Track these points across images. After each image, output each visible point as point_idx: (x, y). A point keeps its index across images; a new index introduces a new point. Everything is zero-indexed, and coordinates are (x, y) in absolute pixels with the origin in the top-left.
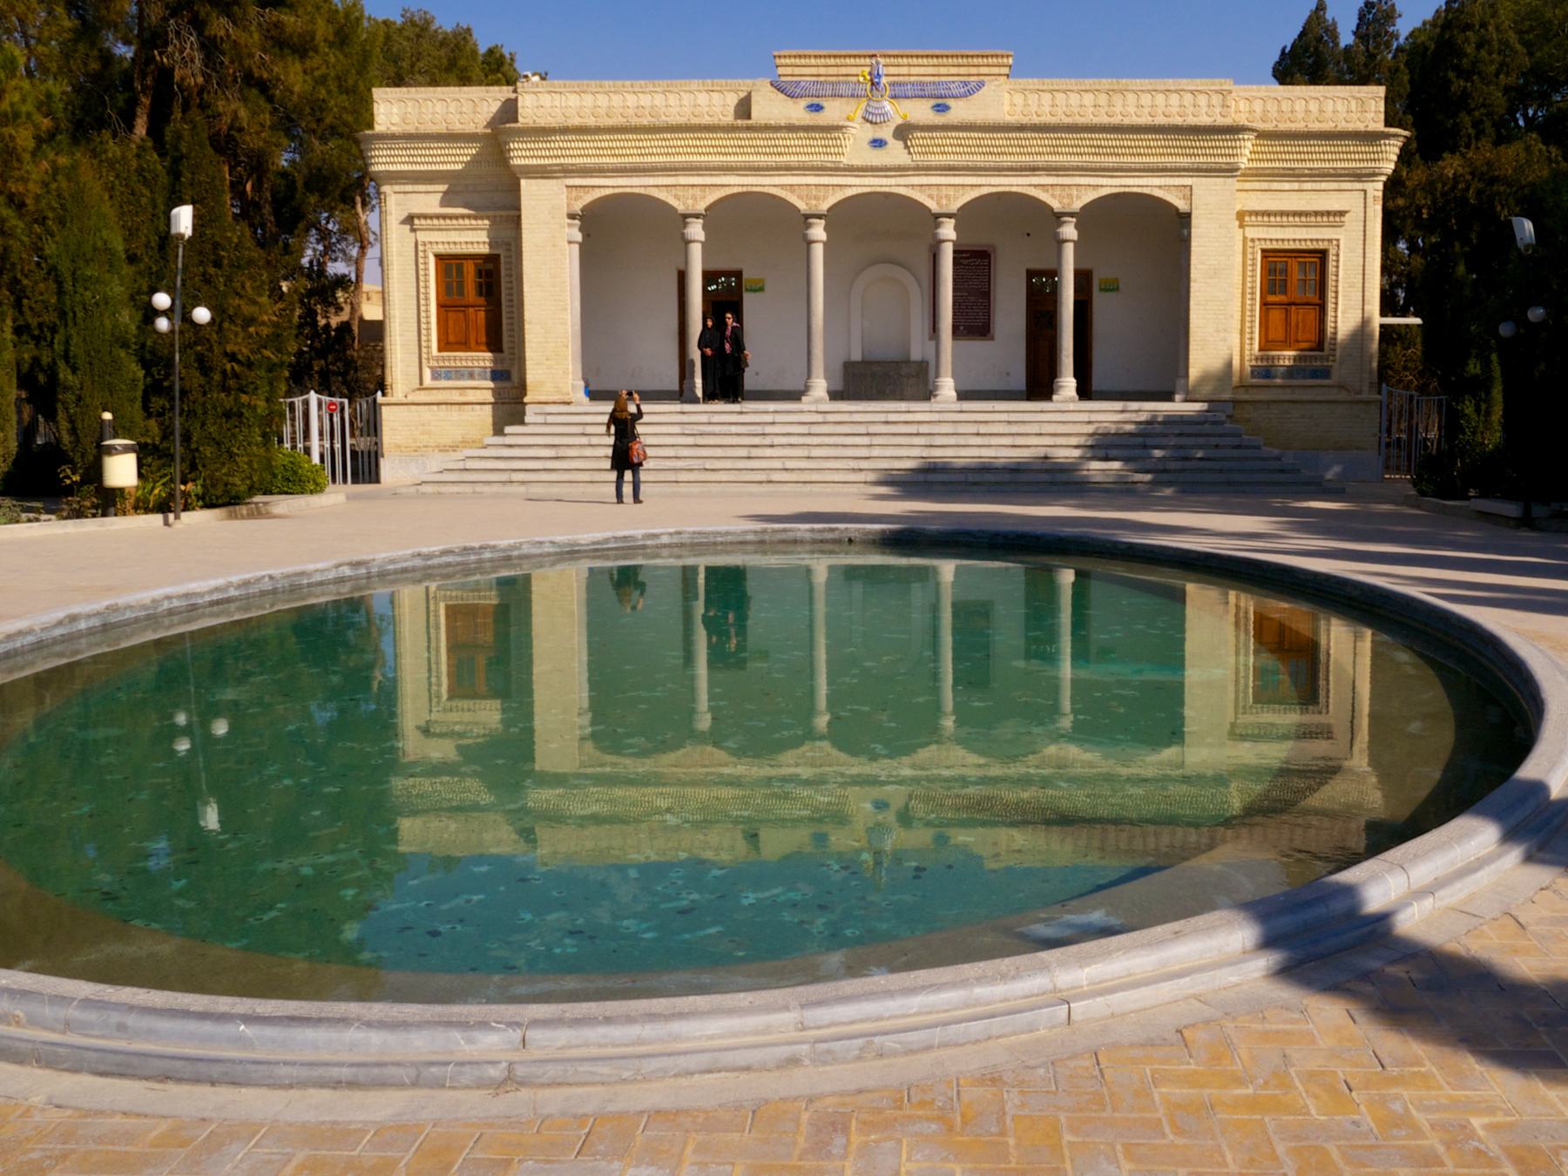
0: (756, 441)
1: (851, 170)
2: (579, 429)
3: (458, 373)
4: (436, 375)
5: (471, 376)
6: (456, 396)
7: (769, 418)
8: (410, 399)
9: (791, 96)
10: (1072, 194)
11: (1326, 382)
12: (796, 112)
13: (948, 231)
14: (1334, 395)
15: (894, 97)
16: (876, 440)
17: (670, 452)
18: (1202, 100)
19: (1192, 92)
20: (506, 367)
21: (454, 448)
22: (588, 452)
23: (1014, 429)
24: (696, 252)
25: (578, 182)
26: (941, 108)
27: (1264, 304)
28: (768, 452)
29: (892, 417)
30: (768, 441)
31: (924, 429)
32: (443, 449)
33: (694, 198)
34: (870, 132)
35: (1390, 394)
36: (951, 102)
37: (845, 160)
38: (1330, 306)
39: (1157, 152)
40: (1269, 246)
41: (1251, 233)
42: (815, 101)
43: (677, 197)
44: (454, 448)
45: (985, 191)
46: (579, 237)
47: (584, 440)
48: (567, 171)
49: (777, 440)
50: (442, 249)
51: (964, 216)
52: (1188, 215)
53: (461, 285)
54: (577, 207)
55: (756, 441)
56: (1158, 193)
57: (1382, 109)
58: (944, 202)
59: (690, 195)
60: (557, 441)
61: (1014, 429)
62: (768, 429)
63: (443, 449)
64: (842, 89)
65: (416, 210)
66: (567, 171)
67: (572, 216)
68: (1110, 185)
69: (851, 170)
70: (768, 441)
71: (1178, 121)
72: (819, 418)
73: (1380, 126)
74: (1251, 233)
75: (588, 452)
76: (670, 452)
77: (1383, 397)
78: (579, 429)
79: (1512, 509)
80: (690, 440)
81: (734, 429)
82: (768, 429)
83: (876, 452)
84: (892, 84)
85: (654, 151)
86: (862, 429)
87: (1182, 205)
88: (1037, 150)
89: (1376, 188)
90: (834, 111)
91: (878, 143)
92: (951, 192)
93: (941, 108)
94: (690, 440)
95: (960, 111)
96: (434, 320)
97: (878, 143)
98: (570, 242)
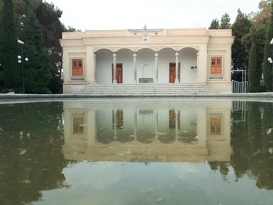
0: (126, 89)
1: (141, 44)
2: (96, 87)
4: (72, 80)
5: (78, 80)
6: (75, 83)
7: (128, 86)
8: (68, 83)
11: (222, 79)
12: (132, 34)
14: (224, 82)
15: (148, 32)
16: (146, 89)
17: (111, 91)
19: (199, 30)
20: (84, 78)
22: (97, 91)
23: (169, 87)
24: (115, 58)
25: (96, 47)
28: (128, 91)
29: (148, 85)
30: (127, 89)
31: (154, 87)
33: (115, 50)
35: (233, 82)
36: (158, 33)
37: (140, 43)
38: (222, 67)
40: (212, 56)
41: (209, 54)
42: (135, 33)
43: (112, 49)
45: (164, 48)
46: (95, 56)
47: (97, 89)
48: (94, 45)
49: (129, 89)
50: (73, 59)
52: (199, 51)
53: (76, 65)
54: (95, 51)
55: (126, 89)
56: (193, 47)
57: (231, 33)
58: (157, 50)
60: (92, 89)
61: (169, 87)
62: (128, 87)
64: (140, 31)
65: (69, 52)
67: (94, 53)
69: (141, 44)
70: (127, 89)
72: (136, 85)
73: (231, 36)
74: (209, 54)
75: (97, 91)
76: (111, 91)
77: (232, 82)
78: (96, 87)
80: (115, 89)
81: (122, 87)
82: (128, 87)
83: (146, 91)
84: (148, 30)
86: (143, 87)
87: (197, 49)
89: (230, 46)
91: (146, 40)
92: (158, 48)
94: (115, 89)
96: (71, 70)
97: (146, 40)
98: (94, 57)
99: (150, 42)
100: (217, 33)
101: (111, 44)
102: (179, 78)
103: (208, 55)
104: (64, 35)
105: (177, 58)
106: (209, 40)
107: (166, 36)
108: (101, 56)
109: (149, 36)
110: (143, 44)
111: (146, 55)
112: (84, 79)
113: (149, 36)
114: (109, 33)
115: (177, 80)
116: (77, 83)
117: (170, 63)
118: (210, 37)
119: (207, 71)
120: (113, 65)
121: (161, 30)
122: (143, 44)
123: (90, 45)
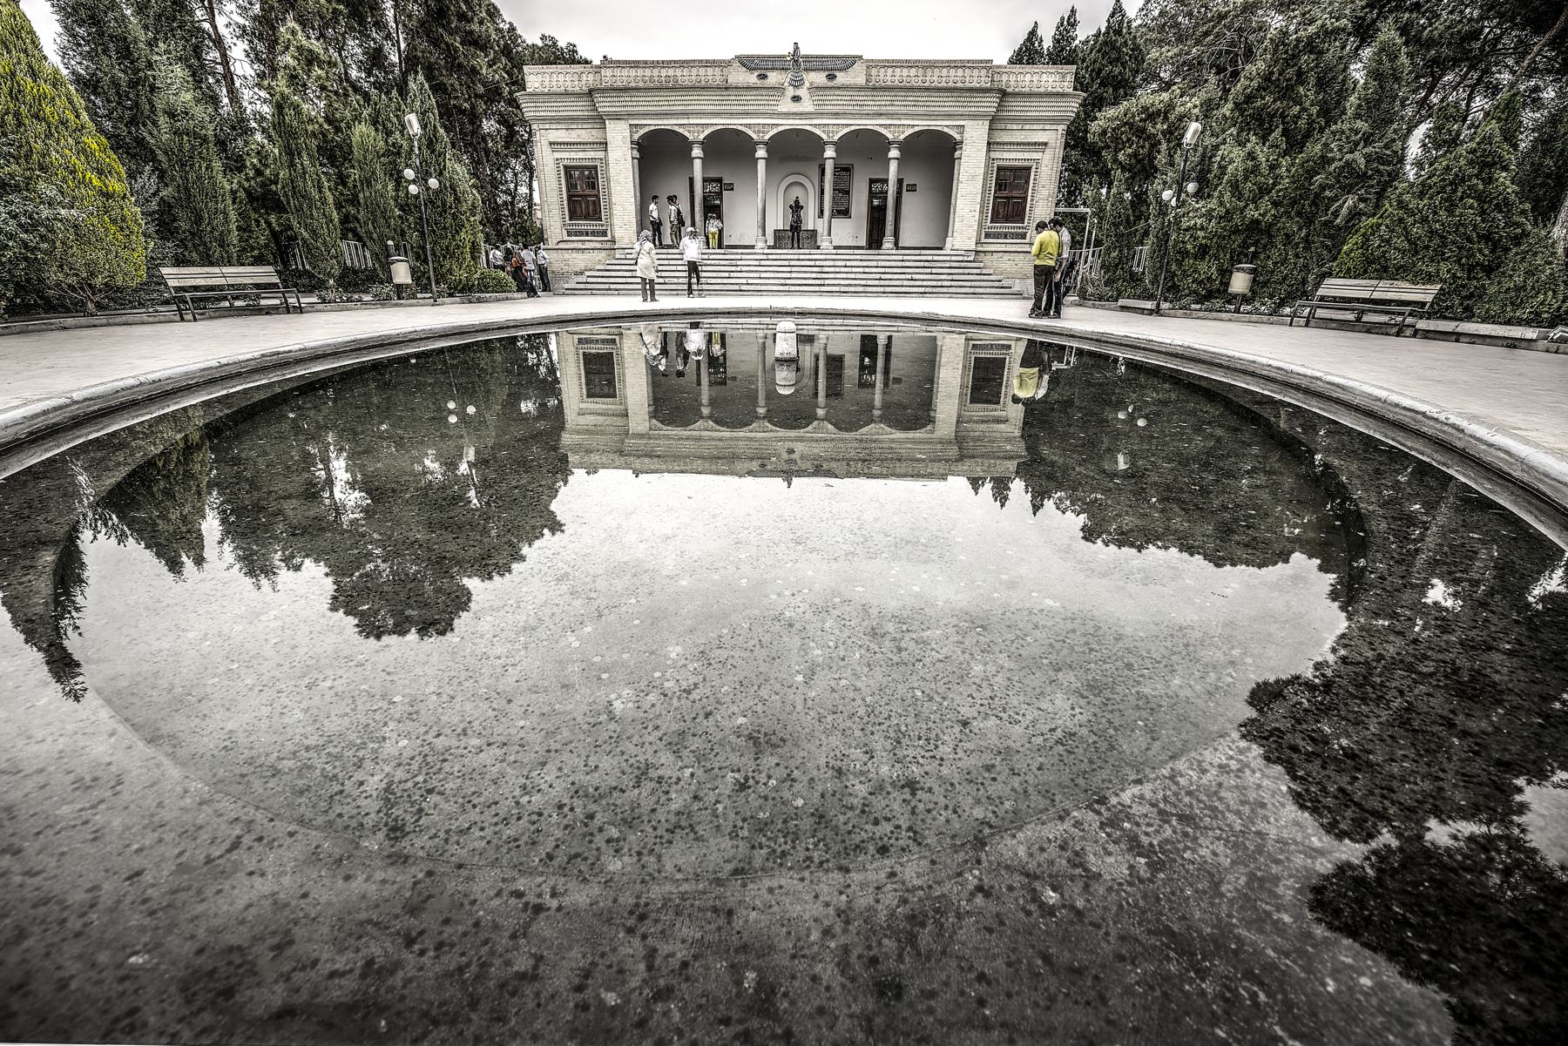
3: (580, 233)
9: (751, 69)
10: (898, 129)
12: (752, 79)
13: (830, 152)
18: (976, 72)
21: (582, 273)
24: (698, 164)
26: (831, 77)
27: (995, 198)
32: (576, 274)
34: (791, 92)
39: (947, 104)
40: (1001, 163)
41: (993, 155)
44: (582, 273)
48: (631, 115)
50: (566, 163)
51: (839, 145)
54: (636, 137)
59: (696, 129)
63: (576, 274)
64: (778, 64)
66: (631, 115)
68: (922, 124)
71: (959, 85)
74: (993, 155)
79: (1149, 305)
85: (677, 102)
87: (958, 137)
88: (882, 102)
89: (1062, 128)
90: (774, 78)
91: (796, 99)
93: (831, 77)
95: (841, 78)
99: (811, 109)
100: (1028, 77)
101: (686, 114)
102: (896, 234)
103: (988, 158)
104: (536, 78)
105: (893, 166)
106: (1000, 107)
107: (861, 88)
108: (658, 153)
109: (807, 84)
110: (787, 115)
111: (794, 150)
112: (604, 234)
113: (807, 84)
114: (679, 72)
115: (888, 242)
116: (587, 245)
117: (872, 181)
118: (1004, 94)
119: (981, 212)
120: (691, 180)
121: (848, 62)
122: (787, 115)
123: (617, 117)
